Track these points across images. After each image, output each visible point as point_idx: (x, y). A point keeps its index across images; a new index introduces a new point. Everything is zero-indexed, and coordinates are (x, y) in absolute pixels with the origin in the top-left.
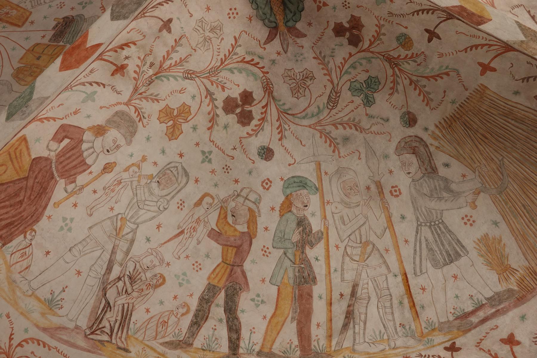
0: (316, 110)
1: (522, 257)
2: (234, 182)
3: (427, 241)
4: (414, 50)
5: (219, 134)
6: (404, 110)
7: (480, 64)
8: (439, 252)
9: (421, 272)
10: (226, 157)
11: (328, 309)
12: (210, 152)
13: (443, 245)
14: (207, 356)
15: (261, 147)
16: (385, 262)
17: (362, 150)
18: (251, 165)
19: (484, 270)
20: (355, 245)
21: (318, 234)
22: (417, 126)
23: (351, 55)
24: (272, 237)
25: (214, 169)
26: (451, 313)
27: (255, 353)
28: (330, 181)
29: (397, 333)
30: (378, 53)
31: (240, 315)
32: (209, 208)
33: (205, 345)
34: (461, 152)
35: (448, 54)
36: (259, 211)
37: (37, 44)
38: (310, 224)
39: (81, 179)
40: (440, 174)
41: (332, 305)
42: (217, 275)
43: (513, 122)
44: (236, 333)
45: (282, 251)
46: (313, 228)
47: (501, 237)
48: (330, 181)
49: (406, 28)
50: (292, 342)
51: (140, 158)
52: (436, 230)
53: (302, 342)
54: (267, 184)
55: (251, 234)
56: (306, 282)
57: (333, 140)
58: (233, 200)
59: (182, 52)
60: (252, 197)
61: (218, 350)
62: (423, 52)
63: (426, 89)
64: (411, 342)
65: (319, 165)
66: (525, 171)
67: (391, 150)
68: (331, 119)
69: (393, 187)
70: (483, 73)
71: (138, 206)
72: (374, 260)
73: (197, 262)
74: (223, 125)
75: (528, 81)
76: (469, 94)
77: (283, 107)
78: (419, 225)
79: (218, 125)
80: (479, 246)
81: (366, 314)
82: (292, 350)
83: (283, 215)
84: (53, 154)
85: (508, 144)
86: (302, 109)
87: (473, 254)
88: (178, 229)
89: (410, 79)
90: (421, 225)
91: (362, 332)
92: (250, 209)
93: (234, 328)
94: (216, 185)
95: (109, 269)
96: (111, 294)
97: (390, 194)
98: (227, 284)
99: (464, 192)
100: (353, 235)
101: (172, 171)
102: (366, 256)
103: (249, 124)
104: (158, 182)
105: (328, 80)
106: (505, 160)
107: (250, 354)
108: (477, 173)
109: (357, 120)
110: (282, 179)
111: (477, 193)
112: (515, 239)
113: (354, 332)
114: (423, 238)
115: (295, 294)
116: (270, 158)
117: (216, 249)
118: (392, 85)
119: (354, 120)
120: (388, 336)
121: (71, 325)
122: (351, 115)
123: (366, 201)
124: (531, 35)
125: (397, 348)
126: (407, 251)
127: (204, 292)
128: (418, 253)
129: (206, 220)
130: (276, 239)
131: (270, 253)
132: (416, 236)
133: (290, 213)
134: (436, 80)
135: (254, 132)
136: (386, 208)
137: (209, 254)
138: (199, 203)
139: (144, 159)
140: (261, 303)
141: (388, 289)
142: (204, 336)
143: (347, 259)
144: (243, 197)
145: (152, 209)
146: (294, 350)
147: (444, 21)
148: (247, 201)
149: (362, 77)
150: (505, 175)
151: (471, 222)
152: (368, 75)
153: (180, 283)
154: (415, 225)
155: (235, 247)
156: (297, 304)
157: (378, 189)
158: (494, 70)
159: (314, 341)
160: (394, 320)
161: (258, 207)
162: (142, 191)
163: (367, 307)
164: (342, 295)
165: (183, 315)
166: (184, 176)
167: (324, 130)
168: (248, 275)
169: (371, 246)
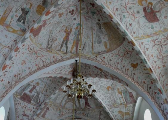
5: (67, 16)
19: (104, 47)
37: (39, 5)
39: (45, 26)
54: (74, 24)
59: (63, 6)
64: (91, 54)
72: (89, 39)
84: (42, 24)
87: (103, 43)
92: (71, 28)
95: (49, 38)
96: (49, 42)
111: (106, 35)
117: (65, 34)
121: (44, 48)
126: (94, 39)
136: (92, 32)
138: (63, 27)
139: (55, 21)
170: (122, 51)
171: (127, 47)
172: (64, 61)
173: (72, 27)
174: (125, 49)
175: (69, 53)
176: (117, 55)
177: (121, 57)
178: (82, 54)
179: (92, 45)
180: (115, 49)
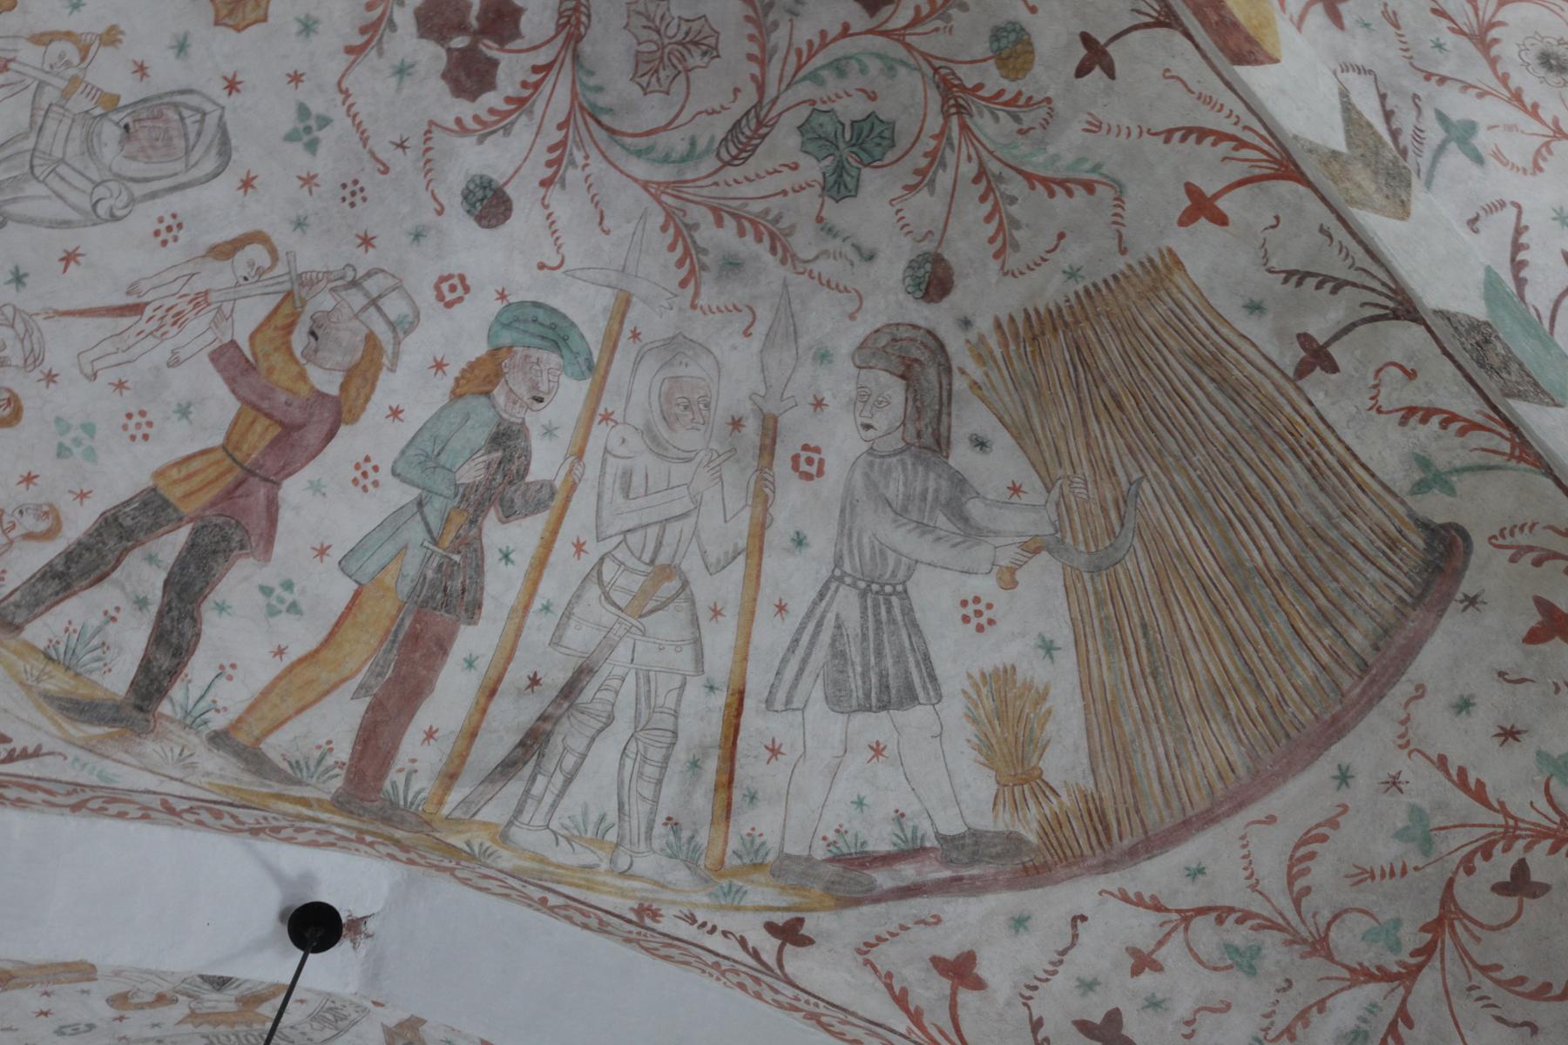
0: (682, 147)
1: (1086, 761)
2: (359, 241)
3: (839, 627)
4: (1027, 86)
6: (928, 246)
7: (1191, 190)
8: (859, 669)
9: (788, 701)
10: (366, 156)
11: (477, 703)
12: (325, 122)
13: (879, 654)
14: (51, 677)
15: (481, 177)
16: (697, 642)
17: (765, 314)
18: (429, 216)
20: (631, 562)
21: (539, 491)
22: (945, 303)
23: (846, 31)
24: (404, 443)
25: (315, 176)
26: (824, 838)
27: (205, 731)
28: (637, 362)
29: (649, 837)
30: (926, 56)
31: (208, 613)
32: (251, 280)
33: (62, 648)
34: (1036, 421)
35: (1115, 130)
36: (396, 355)
38: (527, 454)
40: (951, 462)
41: (496, 698)
42: (189, 477)
43: (1211, 387)
44: (174, 655)
45: (416, 492)
46: (533, 467)
47: (1047, 688)
48: (637, 362)
49: (1033, 10)
50: (331, 750)
51: (101, 29)
52: (876, 606)
53: (360, 760)
54: (452, 289)
55: (345, 409)
56: (447, 606)
57: (693, 252)
58: (333, 290)
60: (395, 307)
61: (95, 677)
62: (1049, 100)
63: (1014, 210)
64: (680, 875)
65: (624, 303)
66: (1188, 536)
67: (845, 345)
68: (714, 191)
69: (806, 448)
70: (1187, 219)
71: (32, 167)
72: (669, 625)
73: (143, 414)
74: (397, 63)
75: (1299, 283)
76: (1123, 267)
77: (592, 96)
78: (836, 579)
79: (381, 53)
80: (978, 692)
81: (583, 757)
82: (321, 769)
83: (461, 396)
85: (1174, 447)
86: (645, 129)
87: (953, 708)
88: (128, 293)
89: (981, 164)
90: (841, 580)
91: (549, 799)
92: (371, 340)
93: (174, 641)
94: (300, 224)
97: (790, 463)
98: (208, 513)
99: (997, 533)
100: (639, 534)
101: (182, 119)
102: (651, 605)
103: (473, 96)
104: (126, 127)
105: (753, 77)
106: (1145, 485)
107: (191, 728)
108: (1055, 493)
109: (784, 224)
110: (502, 296)
111: (1033, 548)
112: (1086, 707)
113: (527, 792)
114: (831, 616)
115: (399, 626)
116: (493, 222)
118: (923, 162)
119: (776, 220)
120: (621, 837)
122: (776, 204)
123: (715, 455)
124: (1366, 144)
125: (632, 877)
126: (771, 635)
127: (127, 503)
128: (800, 651)
129: (227, 308)
130: (411, 452)
131: (376, 483)
132: (815, 604)
133: (483, 399)
134: (1052, 194)
135: (477, 127)
136: (762, 498)
137: (192, 409)
138: (225, 251)
139: (111, 37)
140: (288, 611)
141: (675, 715)
142: (70, 623)
143: (594, 592)
144: (367, 294)
145: (73, 196)
146: (327, 770)
147: (1147, 26)
148: (372, 310)
149: (854, 108)
150: (1130, 525)
151: (983, 620)
152: (869, 107)
153: (61, 445)
154: (825, 573)
155: (281, 423)
156: (394, 655)
157: (764, 435)
158: (1221, 219)
159: (401, 770)
160: (656, 801)
161: (397, 343)
162: (64, 127)
163: (593, 739)
164: (535, 681)
165: (29, 536)
166: (214, 151)
167: (681, 214)
168: (285, 517)
169: (675, 584)
170: (1386, 851)
171: (1509, 734)
172: (19, 803)
173: (400, 328)
174: (1461, 800)
175: (196, 743)
176: (1272, 944)
177: (1359, 975)
178: (480, 839)
179: (714, 729)
180: (1209, 818)
